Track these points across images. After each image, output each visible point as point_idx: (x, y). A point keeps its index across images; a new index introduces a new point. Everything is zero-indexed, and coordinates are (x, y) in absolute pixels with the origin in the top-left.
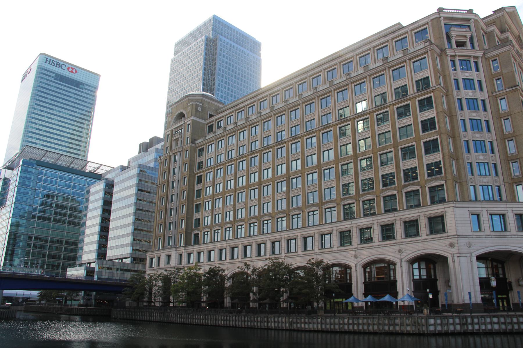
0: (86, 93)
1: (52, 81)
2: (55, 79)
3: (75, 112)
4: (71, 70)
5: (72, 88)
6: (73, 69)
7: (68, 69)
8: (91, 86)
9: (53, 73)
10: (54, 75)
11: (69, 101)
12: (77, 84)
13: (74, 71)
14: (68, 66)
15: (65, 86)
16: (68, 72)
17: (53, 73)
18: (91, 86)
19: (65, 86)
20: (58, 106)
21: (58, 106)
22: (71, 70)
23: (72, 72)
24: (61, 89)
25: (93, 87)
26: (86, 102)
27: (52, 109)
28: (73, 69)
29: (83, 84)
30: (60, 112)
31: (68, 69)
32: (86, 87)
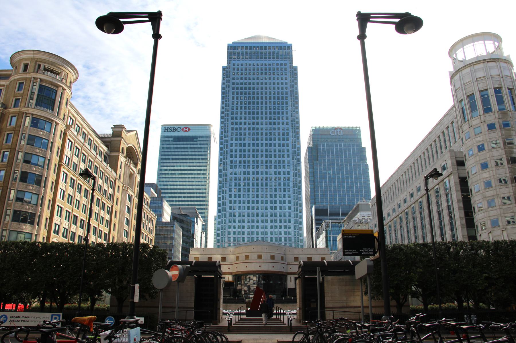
1: (171, 144)
2: (174, 142)
3: (193, 163)
4: (185, 129)
5: (188, 144)
6: (186, 128)
7: (183, 130)
8: (204, 137)
9: (171, 137)
10: (172, 139)
11: (187, 155)
12: (191, 139)
13: (187, 129)
14: (182, 127)
15: (182, 144)
17: (171, 137)
18: (204, 137)
19: (182, 144)
20: (178, 163)
21: (178, 163)
22: (185, 129)
23: (186, 131)
24: (179, 148)
25: (205, 137)
26: (201, 152)
27: (174, 166)
28: (186, 128)
29: (196, 138)
30: (180, 166)
32: (199, 139)
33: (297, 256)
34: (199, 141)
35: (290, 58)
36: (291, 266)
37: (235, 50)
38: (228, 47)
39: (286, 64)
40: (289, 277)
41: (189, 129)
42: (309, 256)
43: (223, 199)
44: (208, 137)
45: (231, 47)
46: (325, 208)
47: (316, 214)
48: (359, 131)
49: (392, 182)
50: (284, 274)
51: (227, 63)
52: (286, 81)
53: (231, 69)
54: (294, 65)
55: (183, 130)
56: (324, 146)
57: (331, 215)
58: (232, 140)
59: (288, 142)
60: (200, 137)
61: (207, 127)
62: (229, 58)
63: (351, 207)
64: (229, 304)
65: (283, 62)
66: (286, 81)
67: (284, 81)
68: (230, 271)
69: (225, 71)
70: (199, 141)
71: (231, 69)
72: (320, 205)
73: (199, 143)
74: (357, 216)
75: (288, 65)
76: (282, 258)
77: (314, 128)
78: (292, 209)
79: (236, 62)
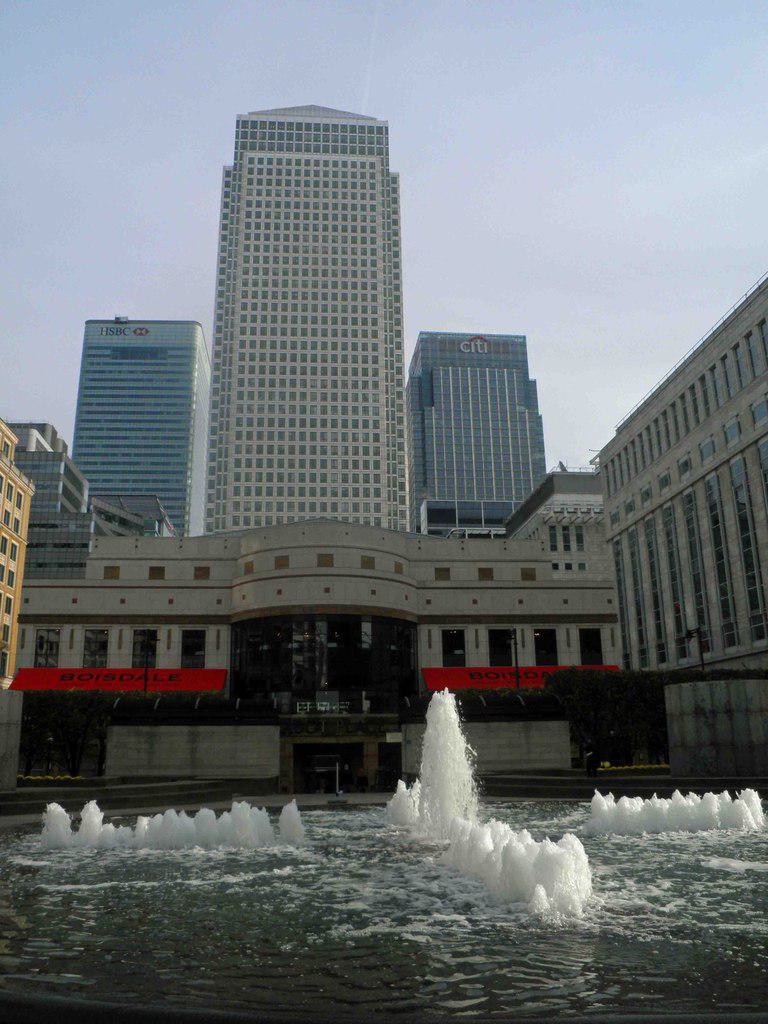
0: (173, 365)
4: (139, 331)
9: (106, 348)
12: (153, 353)
14: (134, 327)
16: (134, 337)
17: (106, 348)
22: (139, 331)
28: (142, 328)
31: (135, 332)
32: (170, 353)
33: (446, 565)
34: (172, 356)
35: (383, 153)
36: (429, 594)
37: (251, 132)
38: (238, 122)
39: (372, 165)
40: (423, 630)
41: (147, 331)
42: (484, 565)
43: (220, 470)
44: (186, 349)
45: (245, 123)
46: (448, 507)
47: (430, 520)
48: (524, 345)
49: (679, 387)
50: (409, 618)
51: (236, 159)
52: (374, 203)
53: (245, 172)
54: (392, 169)
55: (135, 332)
56: (446, 373)
57: (465, 521)
58: (243, 332)
59: (375, 341)
60: (173, 349)
61: (188, 326)
62: (241, 147)
63: (507, 506)
64: (202, 729)
65: (368, 159)
66: (374, 203)
67: (368, 202)
68: (222, 611)
69: (231, 177)
70: (172, 356)
71: (245, 172)
72: (438, 499)
73: (169, 361)
74: (547, 503)
75: (379, 167)
76: (398, 569)
77: (424, 336)
78: (384, 494)
79: (257, 155)
